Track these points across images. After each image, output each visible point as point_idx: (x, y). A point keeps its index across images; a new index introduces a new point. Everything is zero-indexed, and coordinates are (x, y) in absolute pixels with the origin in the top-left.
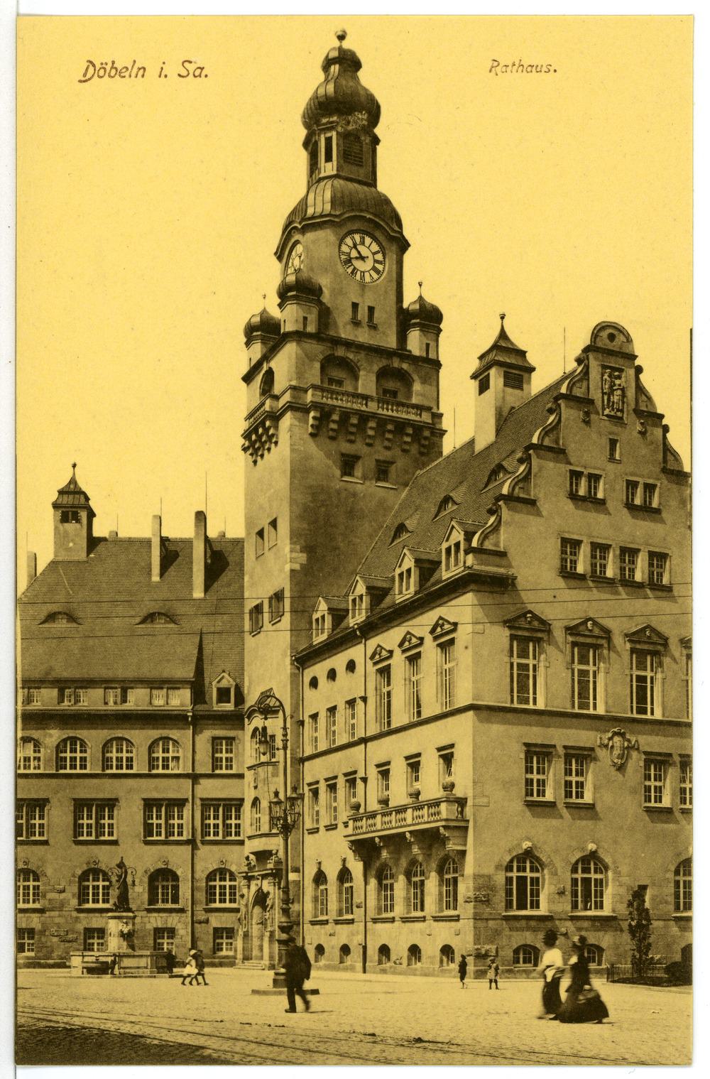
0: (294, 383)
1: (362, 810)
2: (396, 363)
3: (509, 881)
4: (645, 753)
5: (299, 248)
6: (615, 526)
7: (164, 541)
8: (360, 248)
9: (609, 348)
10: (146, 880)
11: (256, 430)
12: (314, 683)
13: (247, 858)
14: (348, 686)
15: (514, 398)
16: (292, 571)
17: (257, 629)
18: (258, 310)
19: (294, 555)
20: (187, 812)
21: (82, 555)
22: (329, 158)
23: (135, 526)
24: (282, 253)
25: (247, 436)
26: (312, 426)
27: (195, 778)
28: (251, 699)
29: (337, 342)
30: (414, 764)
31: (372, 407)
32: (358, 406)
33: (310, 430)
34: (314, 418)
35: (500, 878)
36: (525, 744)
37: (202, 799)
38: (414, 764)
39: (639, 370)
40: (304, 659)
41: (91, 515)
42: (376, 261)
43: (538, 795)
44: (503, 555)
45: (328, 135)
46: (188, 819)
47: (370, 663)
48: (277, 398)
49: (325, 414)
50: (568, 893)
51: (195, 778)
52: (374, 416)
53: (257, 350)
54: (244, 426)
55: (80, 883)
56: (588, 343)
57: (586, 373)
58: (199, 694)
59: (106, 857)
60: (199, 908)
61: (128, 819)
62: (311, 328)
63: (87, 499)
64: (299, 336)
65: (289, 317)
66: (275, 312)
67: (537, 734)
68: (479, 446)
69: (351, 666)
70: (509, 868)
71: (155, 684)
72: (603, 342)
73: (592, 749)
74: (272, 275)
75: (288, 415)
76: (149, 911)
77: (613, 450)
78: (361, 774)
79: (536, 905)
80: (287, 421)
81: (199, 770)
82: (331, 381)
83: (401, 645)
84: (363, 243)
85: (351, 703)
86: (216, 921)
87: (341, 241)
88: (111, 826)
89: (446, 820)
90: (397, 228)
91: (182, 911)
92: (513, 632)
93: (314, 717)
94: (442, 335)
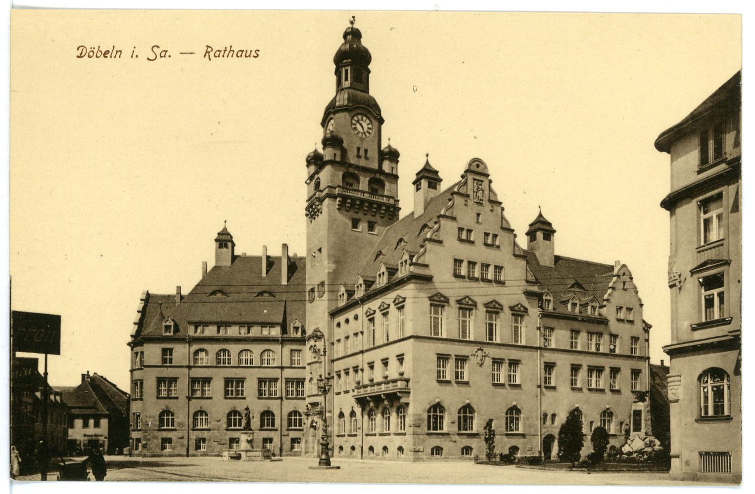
0: (330, 184)
1: (361, 384)
2: (378, 176)
3: (429, 417)
4: (493, 358)
5: (332, 121)
6: (478, 253)
7: (268, 257)
8: (361, 122)
9: (476, 171)
10: (259, 416)
11: (311, 207)
12: (339, 325)
13: (307, 406)
14: (354, 326)
16: (329, 273)
17: (312, 301)
18: (312, 150)
19: (330, 265)
20: (279, 384)
21: (229, 264)
22: (346, 79)
23: (254, 250)
24: (324, 123)
25: (307, 209)
26: (338, 205)
27: (282, 368)
28: (309, 332)
29: (351, 165)
30: (385, 362)
31: (366, 196)
32: (359, 195)
33: (337, 207)
34: (339, 201)
35: (425, 416)
36: (437, 354)
37: (286, 379)
38: (385, 362)
39: (490, 182)
40: (334, 314)
41: (233, 245)
42: (369, 128)
43: (443, 377)
44: (427, 266)
45: (346, 68)
46: (279, 388)
47: (365, 316)
48: (322, 191)
49: (344, 198)
50: (457, 423)
51: (282, 368)
52: (367, 201)
53: (313, 168)
54: (306, 204)
55: (227, 417)
56: (467, 168)
57: (466, 183)
58: (284, 330)
59: (240, 406)
60: (284, 429)
61: (250, 387)
62: (338, 159)
63: (232, 237)
64: (331, 162)
65: (328, 154)
66: (320, 150)
67: (443, 348)
68: (416, 216)
69: (356, 318)
70: (429, 411)
71: (264, 325)
72: (474, 168)
73: (468, 357)
74: (319, 134)
75: (327, 200)
76: (260, 430)
77: (478, 219)
78: (360, 367)
79: (441, 428)
80: (327, 201)
81: (284, 365)
82: (347, 184)
83: (379, 308)
84: (362, 120)
85: (356, 334)
86: (293, 434)
87: (352, 118)
88: (242, 391)
89: (401, 389)
90: (378, 113)
91: (276, 430)
92: (432, 302)
93: (339, 341)
94: (399, 164)
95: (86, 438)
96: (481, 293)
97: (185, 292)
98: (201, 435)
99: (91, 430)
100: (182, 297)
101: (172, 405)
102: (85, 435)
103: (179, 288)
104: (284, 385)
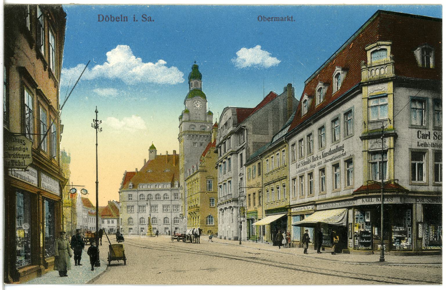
8: (197, 103)
20: (170, 207)
23: (164, 154)
41: (156, 151)
46: (170, 208)
49: (190, 135)
54: (178, 137)
58: (172, 185)
86: (176, 226)
95: (109, 228)
97: (139, 170)
98: (142, 226)
99: (111, 225)
100: (138, 172)
101: (132, 215)
102: (108, 227)
103: (137, 169)
104: (172, 206)
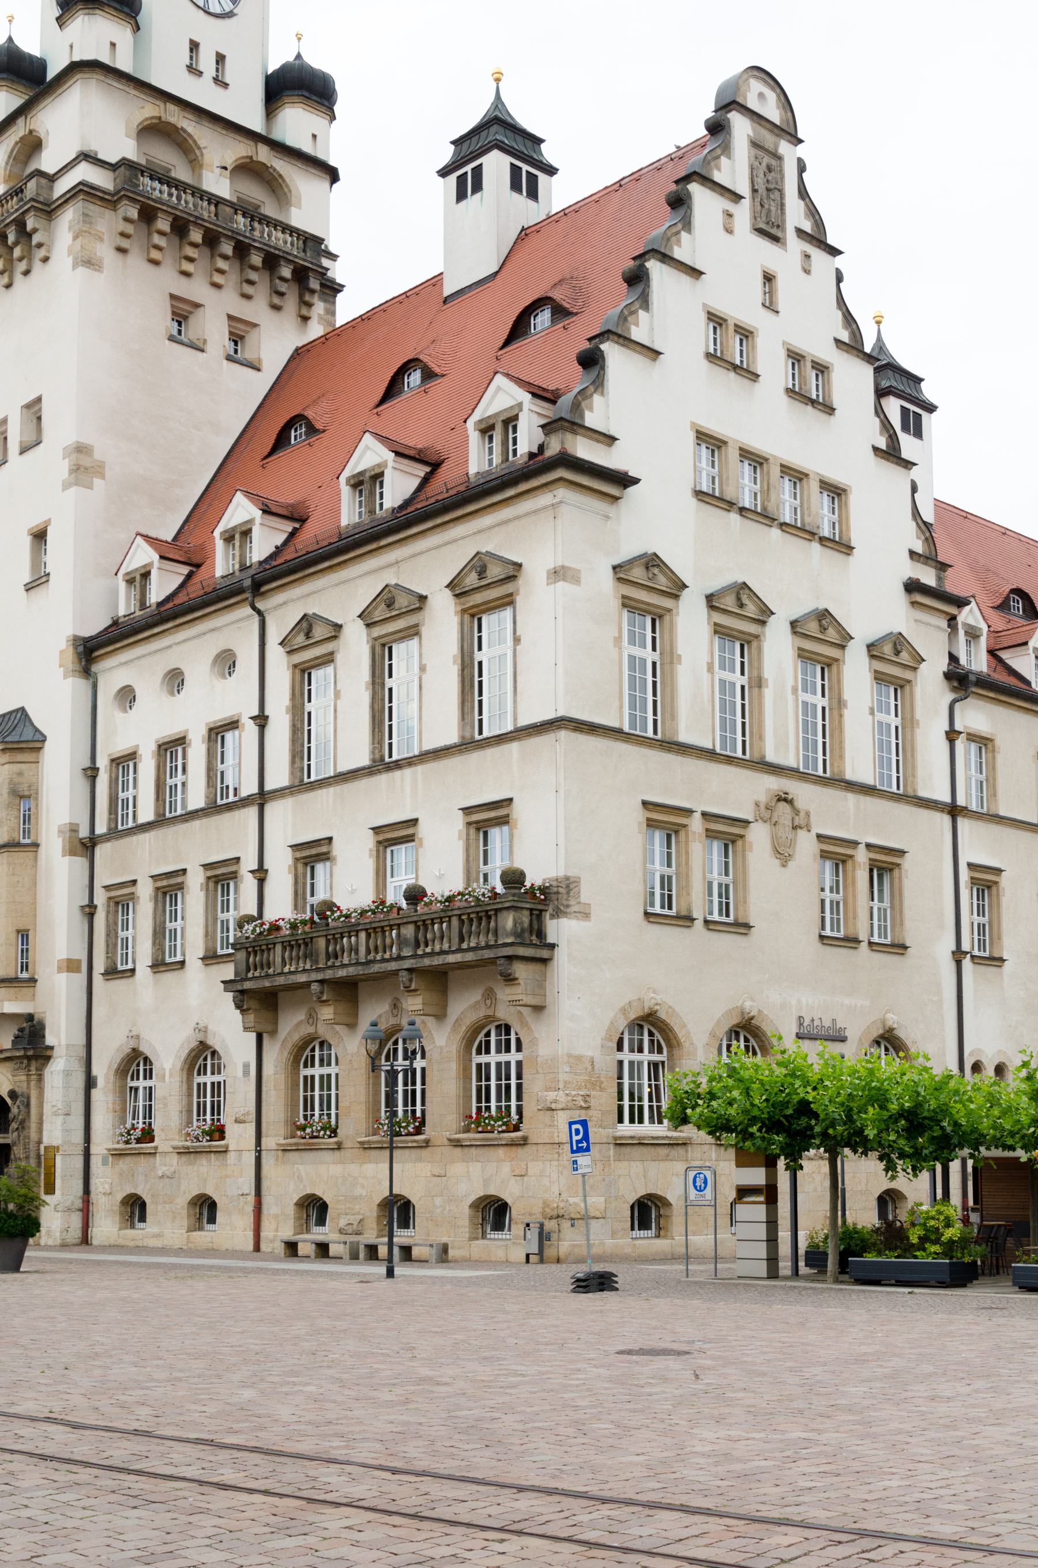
12: (127, 696)
15: (526, 212)
47: (275, 654)
73: (746, 823)
96: (791, 579)
